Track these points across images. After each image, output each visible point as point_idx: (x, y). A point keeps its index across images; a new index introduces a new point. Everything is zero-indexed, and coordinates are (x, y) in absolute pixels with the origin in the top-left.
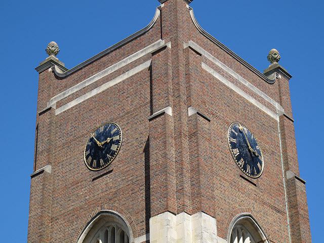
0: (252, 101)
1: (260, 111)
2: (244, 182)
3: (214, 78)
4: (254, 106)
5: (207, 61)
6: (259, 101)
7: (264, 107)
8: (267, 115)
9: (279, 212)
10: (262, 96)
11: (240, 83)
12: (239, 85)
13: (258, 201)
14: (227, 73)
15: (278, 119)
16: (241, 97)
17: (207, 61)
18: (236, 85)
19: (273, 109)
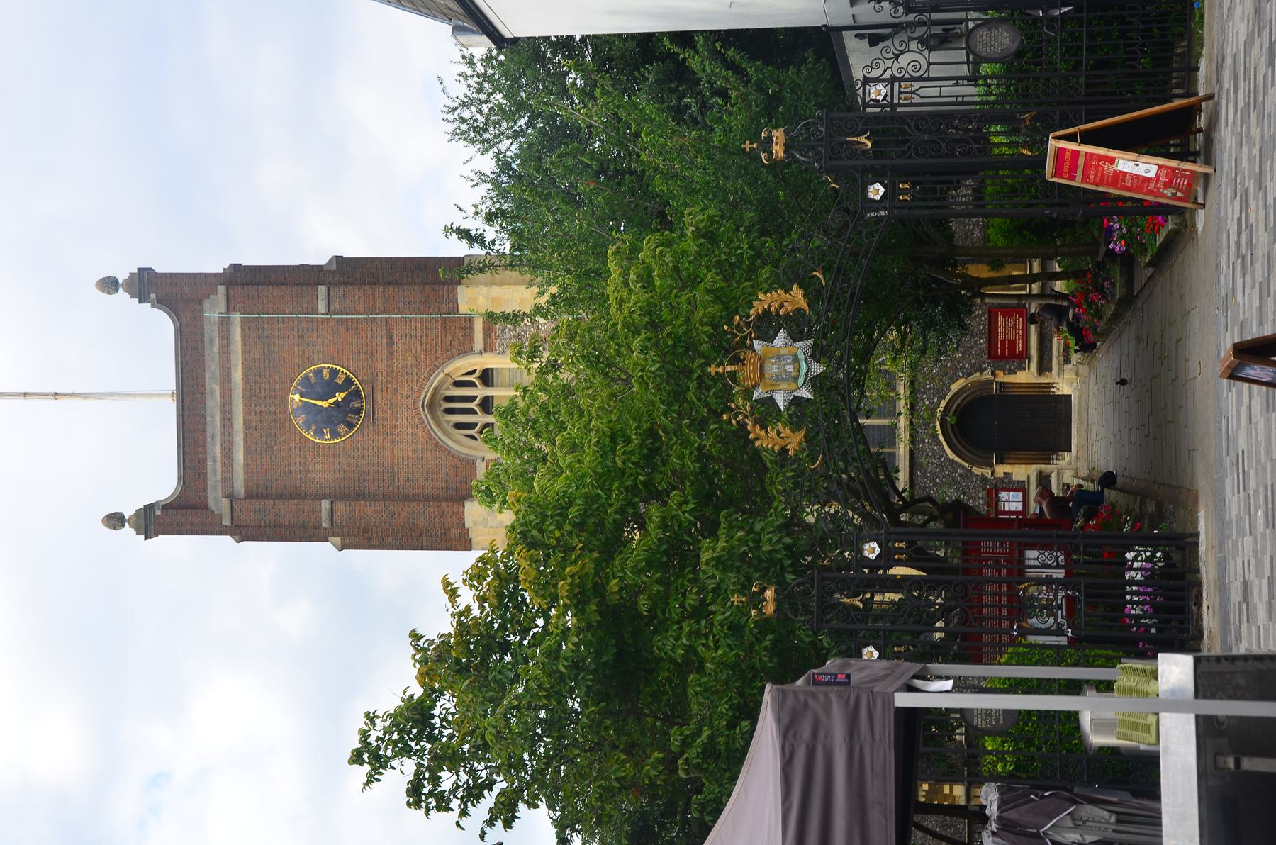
0: (237, 375)
1: (245, 359)
2: (379, 414)
3: (246, 465)
4: (245, 375)
5: (228, 479)
6: (229, 361)
7: (233, 348)
8: (244, 344)
9: (391, 338)
10: (216, 350)
11: (223, 405)
12: (227, 407)
13: (395, 386)
14: (223, 434)
15: (236, 317)
16: (245, 405)
17: (228, 479)
18: (230, 412)
19: (225, 324)
